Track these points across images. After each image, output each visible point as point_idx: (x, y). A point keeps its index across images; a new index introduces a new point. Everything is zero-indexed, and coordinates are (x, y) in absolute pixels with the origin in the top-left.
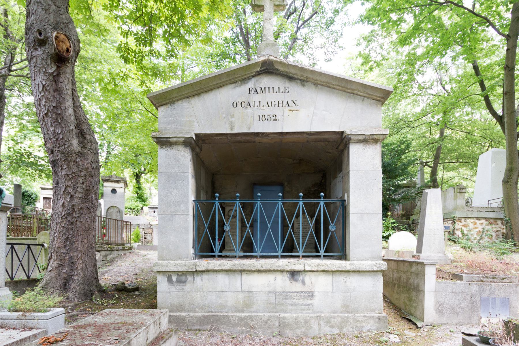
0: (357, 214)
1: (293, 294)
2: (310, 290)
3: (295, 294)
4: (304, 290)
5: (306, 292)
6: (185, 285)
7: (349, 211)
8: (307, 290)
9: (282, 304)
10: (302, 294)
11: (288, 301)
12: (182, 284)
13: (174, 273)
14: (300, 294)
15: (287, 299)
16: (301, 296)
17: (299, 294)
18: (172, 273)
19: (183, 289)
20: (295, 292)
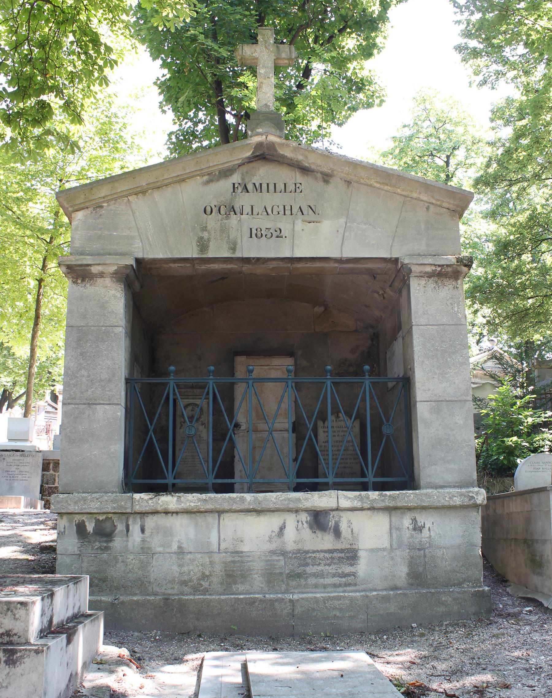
0: (429, 403)
1: (317, 555)
2: (349, 547)
3: (322, 555)
4: (339, 546)
5: (342, 551)
6: (111, 541)
7: (415, 397)
8: (343, 547)
9: (299, 576)
10: (335, 555)
11: (310, 569)
12: (105, 539)
13: (89, 516)
14: (331, 555)
15: (307, 564)
16: (332, 558)
17: (327, 555)
18: (86, 516)
19: (107, 548)
20: (322, 551)
